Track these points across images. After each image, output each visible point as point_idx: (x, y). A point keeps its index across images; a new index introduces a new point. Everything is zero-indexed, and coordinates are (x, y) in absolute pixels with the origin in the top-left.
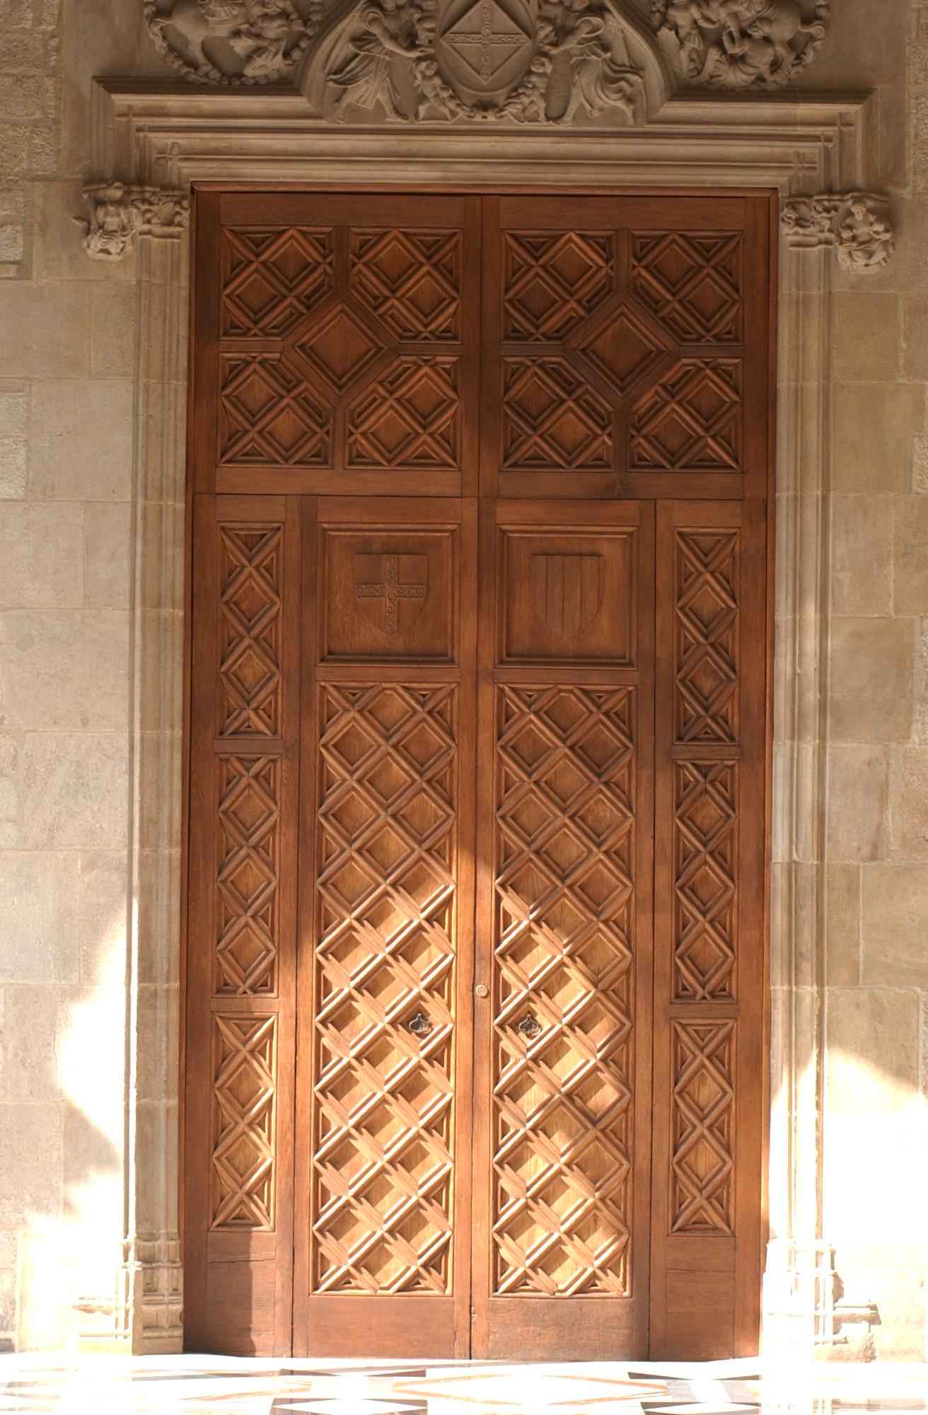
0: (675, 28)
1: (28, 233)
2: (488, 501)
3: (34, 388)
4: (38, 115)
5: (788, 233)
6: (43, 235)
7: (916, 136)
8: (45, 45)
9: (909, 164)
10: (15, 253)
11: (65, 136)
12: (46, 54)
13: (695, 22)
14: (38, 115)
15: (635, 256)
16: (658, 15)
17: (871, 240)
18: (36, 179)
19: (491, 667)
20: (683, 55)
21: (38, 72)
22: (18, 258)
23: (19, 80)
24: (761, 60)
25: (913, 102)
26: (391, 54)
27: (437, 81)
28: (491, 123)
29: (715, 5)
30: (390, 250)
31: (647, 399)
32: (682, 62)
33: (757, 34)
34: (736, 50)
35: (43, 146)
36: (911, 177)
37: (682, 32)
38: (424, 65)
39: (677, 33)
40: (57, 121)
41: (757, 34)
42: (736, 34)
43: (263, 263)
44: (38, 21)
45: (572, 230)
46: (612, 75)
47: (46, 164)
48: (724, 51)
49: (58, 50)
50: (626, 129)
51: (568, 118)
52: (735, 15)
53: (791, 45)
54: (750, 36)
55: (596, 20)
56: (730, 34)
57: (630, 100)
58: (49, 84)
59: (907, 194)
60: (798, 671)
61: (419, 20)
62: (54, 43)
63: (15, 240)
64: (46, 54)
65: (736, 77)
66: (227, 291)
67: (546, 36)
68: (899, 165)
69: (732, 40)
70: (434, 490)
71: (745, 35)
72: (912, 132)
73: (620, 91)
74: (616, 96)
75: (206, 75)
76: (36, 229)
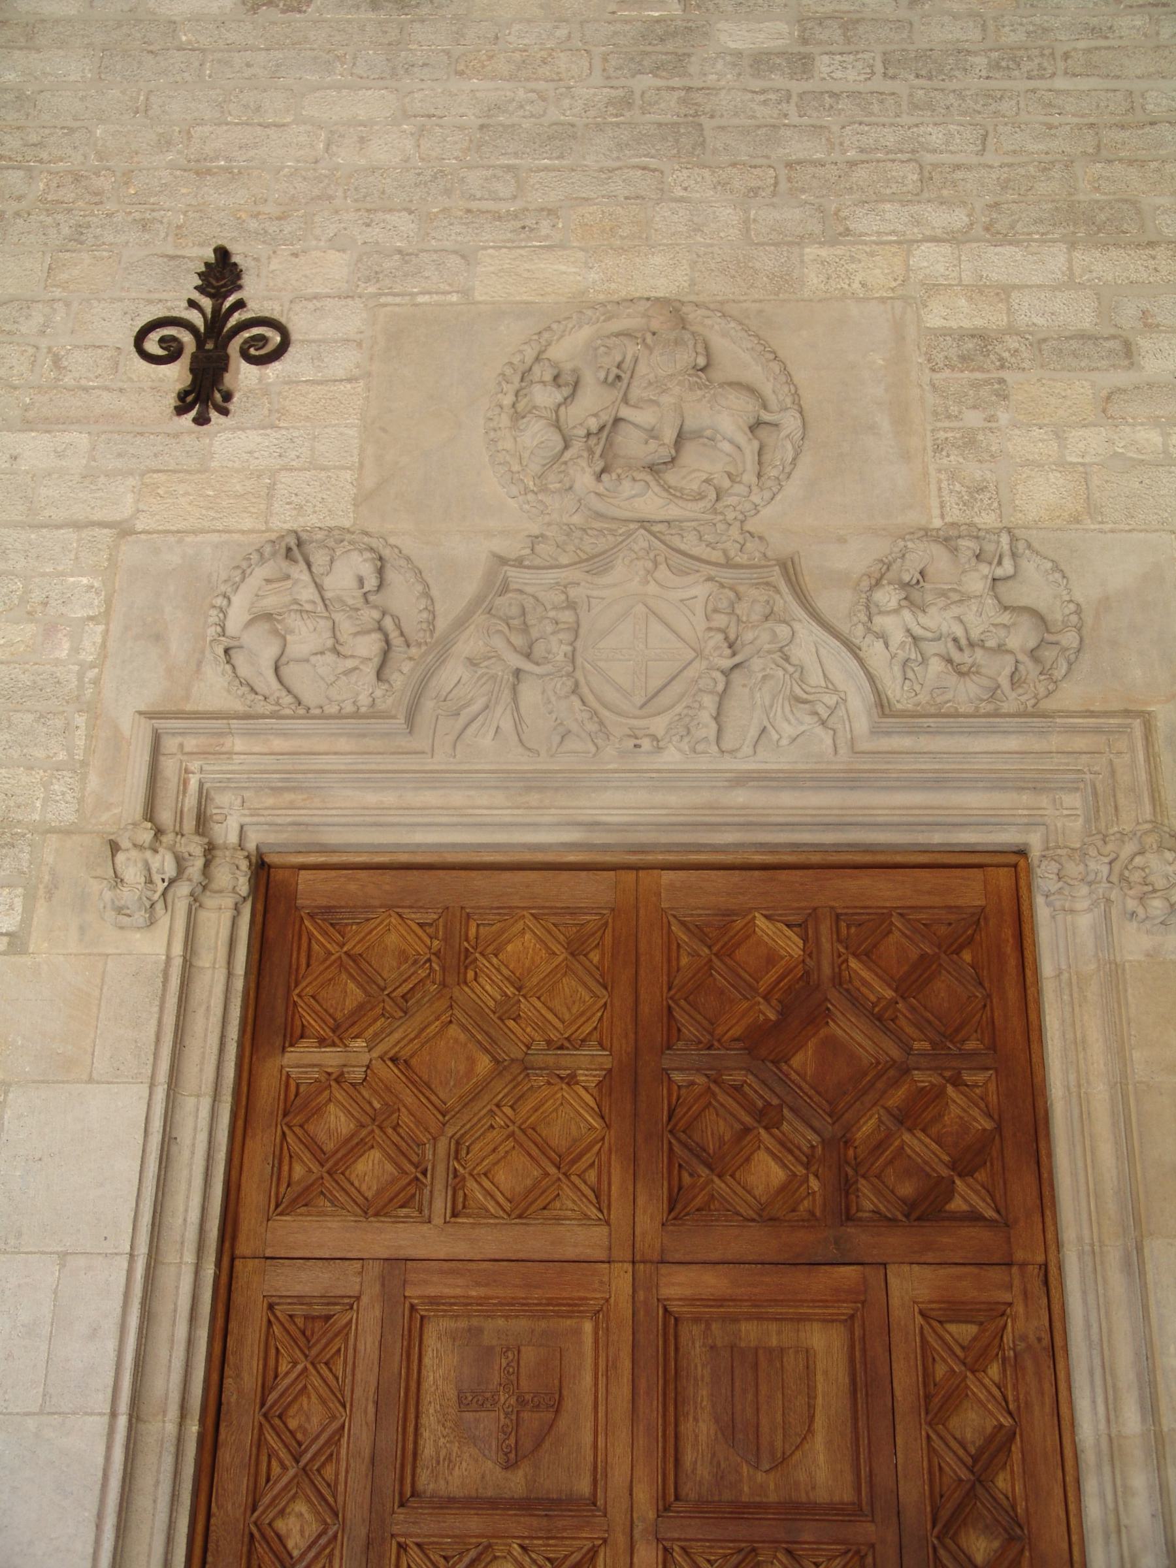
0: (883, 637)
1: (30, 899)
2: (648, 1264)
3: (11, 1095)
4: (62, 756)
6: (50, 896)
8: (81, 676)
10: (9, 923)
11: (94, 781)
14: (62, 756)
16: (860, 626)
18: (52, 831)
19: (652, 1515)
22: (12, 929)
23: (41, 717)
24: (1001, 668)
29: (932, 610)
30: (525, 947)
31: (866, 1128)
35: (63, 794)
39: (887, 645)
40: (84, 764)
44: (75, 649)
45: (756, 909)
46: (805, 696)
47: (65, 813)
49: (96, 682)
55: (783, 631)
56: (955, 640)
58: (80, 720)
60: (1124, 1521)
61: (553, 633)
62: (92, 674)
63: (11, 907)
64: (81, 686)
65: (965, 693)
66: (297, 991)
67: (716, 648)
70: (570, 1253)
74: (808, 719)
76: (41, 892)
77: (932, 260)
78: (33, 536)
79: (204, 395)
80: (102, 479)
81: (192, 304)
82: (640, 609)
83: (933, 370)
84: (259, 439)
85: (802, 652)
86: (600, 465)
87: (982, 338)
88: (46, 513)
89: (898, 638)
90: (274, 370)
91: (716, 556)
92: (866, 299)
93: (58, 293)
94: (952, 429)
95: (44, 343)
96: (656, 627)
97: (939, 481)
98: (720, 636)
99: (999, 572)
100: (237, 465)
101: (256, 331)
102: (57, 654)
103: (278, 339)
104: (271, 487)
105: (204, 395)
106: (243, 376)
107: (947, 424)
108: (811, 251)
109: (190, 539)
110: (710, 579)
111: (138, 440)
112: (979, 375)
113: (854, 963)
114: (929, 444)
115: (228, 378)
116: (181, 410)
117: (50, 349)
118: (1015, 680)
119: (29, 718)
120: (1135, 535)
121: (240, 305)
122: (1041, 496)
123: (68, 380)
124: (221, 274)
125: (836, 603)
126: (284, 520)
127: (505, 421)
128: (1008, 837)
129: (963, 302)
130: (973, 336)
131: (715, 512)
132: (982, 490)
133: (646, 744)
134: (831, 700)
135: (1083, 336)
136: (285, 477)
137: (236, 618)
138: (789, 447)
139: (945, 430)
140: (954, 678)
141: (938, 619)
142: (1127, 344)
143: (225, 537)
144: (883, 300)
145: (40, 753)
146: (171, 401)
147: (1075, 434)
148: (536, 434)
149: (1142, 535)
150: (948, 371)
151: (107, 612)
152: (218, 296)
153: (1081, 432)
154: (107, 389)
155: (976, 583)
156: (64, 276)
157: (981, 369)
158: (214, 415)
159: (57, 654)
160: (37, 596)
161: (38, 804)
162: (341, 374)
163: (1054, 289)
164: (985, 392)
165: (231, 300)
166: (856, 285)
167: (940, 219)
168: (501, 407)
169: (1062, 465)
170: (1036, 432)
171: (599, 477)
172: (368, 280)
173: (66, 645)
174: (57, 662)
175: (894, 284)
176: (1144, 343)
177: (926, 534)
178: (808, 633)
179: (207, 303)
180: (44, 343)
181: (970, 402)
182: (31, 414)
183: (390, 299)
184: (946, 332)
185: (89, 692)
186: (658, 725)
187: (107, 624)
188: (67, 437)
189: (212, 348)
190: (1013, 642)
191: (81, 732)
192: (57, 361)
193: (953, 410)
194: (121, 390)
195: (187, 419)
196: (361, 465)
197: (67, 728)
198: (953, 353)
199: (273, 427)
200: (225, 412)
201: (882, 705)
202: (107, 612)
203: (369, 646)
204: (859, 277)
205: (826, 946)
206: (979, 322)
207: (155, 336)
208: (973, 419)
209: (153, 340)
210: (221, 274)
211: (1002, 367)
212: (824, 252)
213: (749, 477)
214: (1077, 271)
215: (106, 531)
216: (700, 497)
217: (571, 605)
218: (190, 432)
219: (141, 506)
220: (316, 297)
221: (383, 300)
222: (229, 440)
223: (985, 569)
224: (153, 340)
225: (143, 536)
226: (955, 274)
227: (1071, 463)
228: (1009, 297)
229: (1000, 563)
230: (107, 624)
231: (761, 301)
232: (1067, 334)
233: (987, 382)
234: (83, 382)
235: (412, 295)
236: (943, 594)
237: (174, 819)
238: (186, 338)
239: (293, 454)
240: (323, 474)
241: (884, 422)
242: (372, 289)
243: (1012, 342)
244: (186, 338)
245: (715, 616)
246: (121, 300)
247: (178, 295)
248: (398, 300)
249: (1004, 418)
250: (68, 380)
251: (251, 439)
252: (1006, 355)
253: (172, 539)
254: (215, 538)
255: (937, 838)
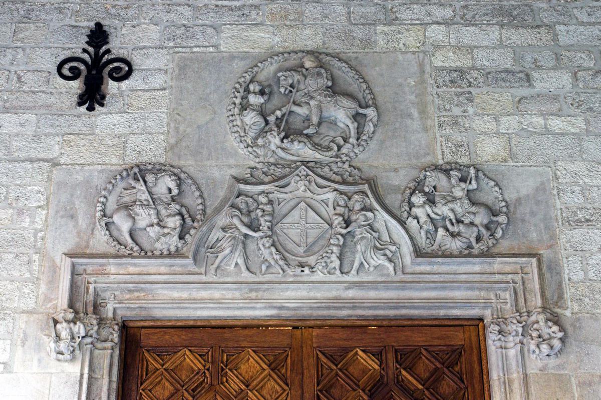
0: (416, 218)
5: (492, 341)
7: (569, 279)
8: (35, 236)
9: (567, 295)
10: (4, 358)
11: (43, 288)
12: (35, 241)
13: (428, 215)
14: (28, 275)
15: (397, 362)
16: (406, 212)
17: (551, 338)
20: (423, 233)
21: (31, 251)
24: (472, 234)
25: (565, 260)
26: (246, 236)
27: (273, 250)
28: (308, 275)
29: (439, 205)
32: (422, 240)
33: (466, 221)
34: (455, 229)
36: (570, 304)
37: (422, 221)
38: (265, 240)
39: (418, 222)
40: (38, 279)
41: (466, 221)
42: (454, 221)
43: (166, 370)
45: (358, 347)
46: (380, 247)
47: (31, 304)
48: (447, 230)
49: (42, 238)
50: (389, 279)
51: (353, 272)
52: (452, 210)
53: (487, 227)
54: (462, 222)
55: (370, 215)
56: (450, 220)
57: (390, 260)
58: (36, 257)
59: (568, 313)
61: (262, 216)
62: (40, 235)
64: (35, 241)
65: (455, 245)
66: (142, 388)
67: (339, 224)
68: (561, 297)
69: (452, 224)
71: (459, 221)
72: (566, 277)
73: (385, 255)
74: (382, 258)
75: (132, 249)
76: (19, 342)
77: (436, 33)
78: (10, 166)
79: (92, 97)
80: (43, 137)
81: (85, 51)
82: (303, 205)
83: (438, 87)
84: (119, 118)
85: (380, 225)
86: (283, 134)
87: (460, 71)
88: (16, 154)
89: (423, 218)
90: (125, 84)
91: (338, 178)
92: (406, 53)
93: (19, 44)
94: (447, 116)
95: (13, 69)
96: (311, 213)
97: (441, 142)
98: (341, 219)
99: (470, 187)
100: (108, 131)
101: (116, 64)
102: (23, 225)
103: (127, 69)
104: (126, 142)
105: (92, 97)
106: (112, 87)
107: (444, 113)
108: (380, 28)
109: (87, 168)
110: (336, 190)
111: (60, 118)
112: (459, 90)
113: (403, 372)
114: (437, 124)
115: (103, 87)
116: (80, 104)
117: (16, 72)
118: (478, 239)
119: (11, 256)
120: (532, 168)
121: (108, 51)
122: (488, 150)
123: (25, 88)
124: (98, 36)
125: (393, 200)
126: (132, 158)
127: (236, 111)
128: (474, 312)
129: (451, 54)
130: (456, 71)
131: (337, 156)
132: (462, 146)
133: (307, 270)
134: (393, 248)
135: (507, 71)
136: (132, 138)
137: (111, 205)
138: (371, 125)
139: (443, 116)
140: (450, 239)
141: (443, 210)
142: (528, 75)
143: (104, 167)
144: (414, 53)
145: (17, 274)
146: (75, 99)
147: (504, 119)
148: (251, 118)
149: (535, 168)
150: (445, 88)
151: (47, 204)
152: (97, 47)
153: (507, 118)
154: (44, 92)
155: (458, 193)
156: (22, 36)
157: (460, 87)
158: (97, 106)
159: (23, 225)
160: (13, 196)
161: (16, 298)
162: (157, 86)
163: (493, 48)
164: (462, 98)
165: (104, 48)
166: (401, 45)
167: (440, 13)
168: (235, 104)
169: (498, 134)
170: (486, 118)
171: (282, 141)
172: (169, 39)
173: (28, 220)
174: (25, 229)
175: (419, 45)
176: (535, 75)
177: (437, 168)
178: (382, 215)
179: (91, 49)
180: (13, 69)
181: (455, 103)
182: (7, 105)
183: (180, 49)
184: (443, 69)
185: (39, 244)
186: (312, 260)
187: (48, 210)
188: (26, 116)
189: (95, 72)
190: (477, 220)
191: (37, 263)
192: (19, 78)
193: (448, 107)
194: (51, 93)
195: (83, 109)
196: (168, 132)
197: (29, 262)
198: (447, 79)
199: (126, 112)
200: (102, 105)
201: (418, 253)
202: (47, 204)
203: (174, 222)
204: (402, 42)
205: (391, 365)
206: (459, 64)
207: (67, 66)
208: (457, 111)
209: (67, 69)
210: (98, 36)
211: (470, 86)
212: (386, 29)
213: (353, 140)
214: (504, 39)
215: (46, 163)
216: (329, 149)
217: (270, 202)
218: (85, 114)
219: (63, 151)
220: (144, 48)
221: (177, 50)
222: (105, 119)
223: (463, 185)
224: (67, 69)
225: (64, 167)
226: (447, 40)
227: (502, 133)
228: (473, 52)
229: (470, 183)
230: (48, 210)
231: (356, 52)
232: (499, 70)
233: (463, 93)
234: (33, 89)
235: (190, 47)
236: (444, 197)
237: (83, 305)
238: (82, 67)
239: (136, 126)
240: (150, 136)
241: (415, 113)
242: (171, 44)
243: (475, 74)
244: (82, 67)
245: (338, 208)
246: (50, 48)
247: (78, 46)
248: (184, 50)
249: (471, 110)
250: (25, 88)
251: (116, 118)
252: (472, 80)
253: (78, 168)
254: (99, 167)
255: (442, 313)
